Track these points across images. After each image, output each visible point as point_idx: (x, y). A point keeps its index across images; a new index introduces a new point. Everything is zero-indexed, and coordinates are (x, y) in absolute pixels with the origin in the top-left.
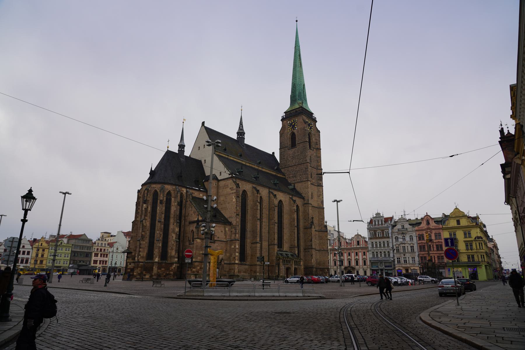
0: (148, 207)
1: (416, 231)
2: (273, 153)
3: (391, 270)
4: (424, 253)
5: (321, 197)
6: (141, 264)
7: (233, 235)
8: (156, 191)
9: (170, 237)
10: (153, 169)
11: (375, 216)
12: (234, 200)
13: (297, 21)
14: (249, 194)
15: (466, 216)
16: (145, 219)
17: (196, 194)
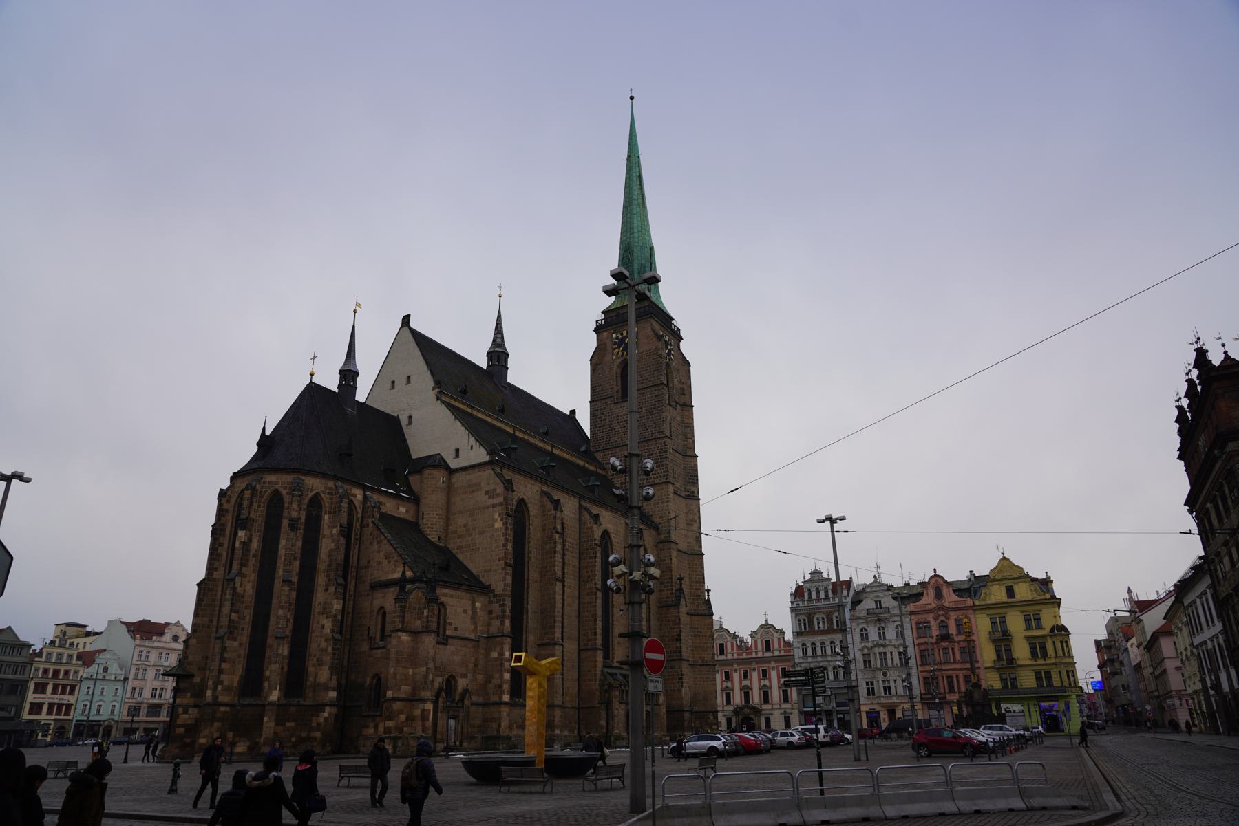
0: (250, 540)
1: (912, 613)
2: (573, 412)
5: (695, 525)
6: (223, 709)
7: (496, 623)
8: (277, 493)
9: (314, 627)
10: (268, 433)
11: (808, 577)
12: (499, 524)
13: (632, 98)
14: (533, 510)
15: (1028, 576)
16: (240, 574)
17: (390, 507)
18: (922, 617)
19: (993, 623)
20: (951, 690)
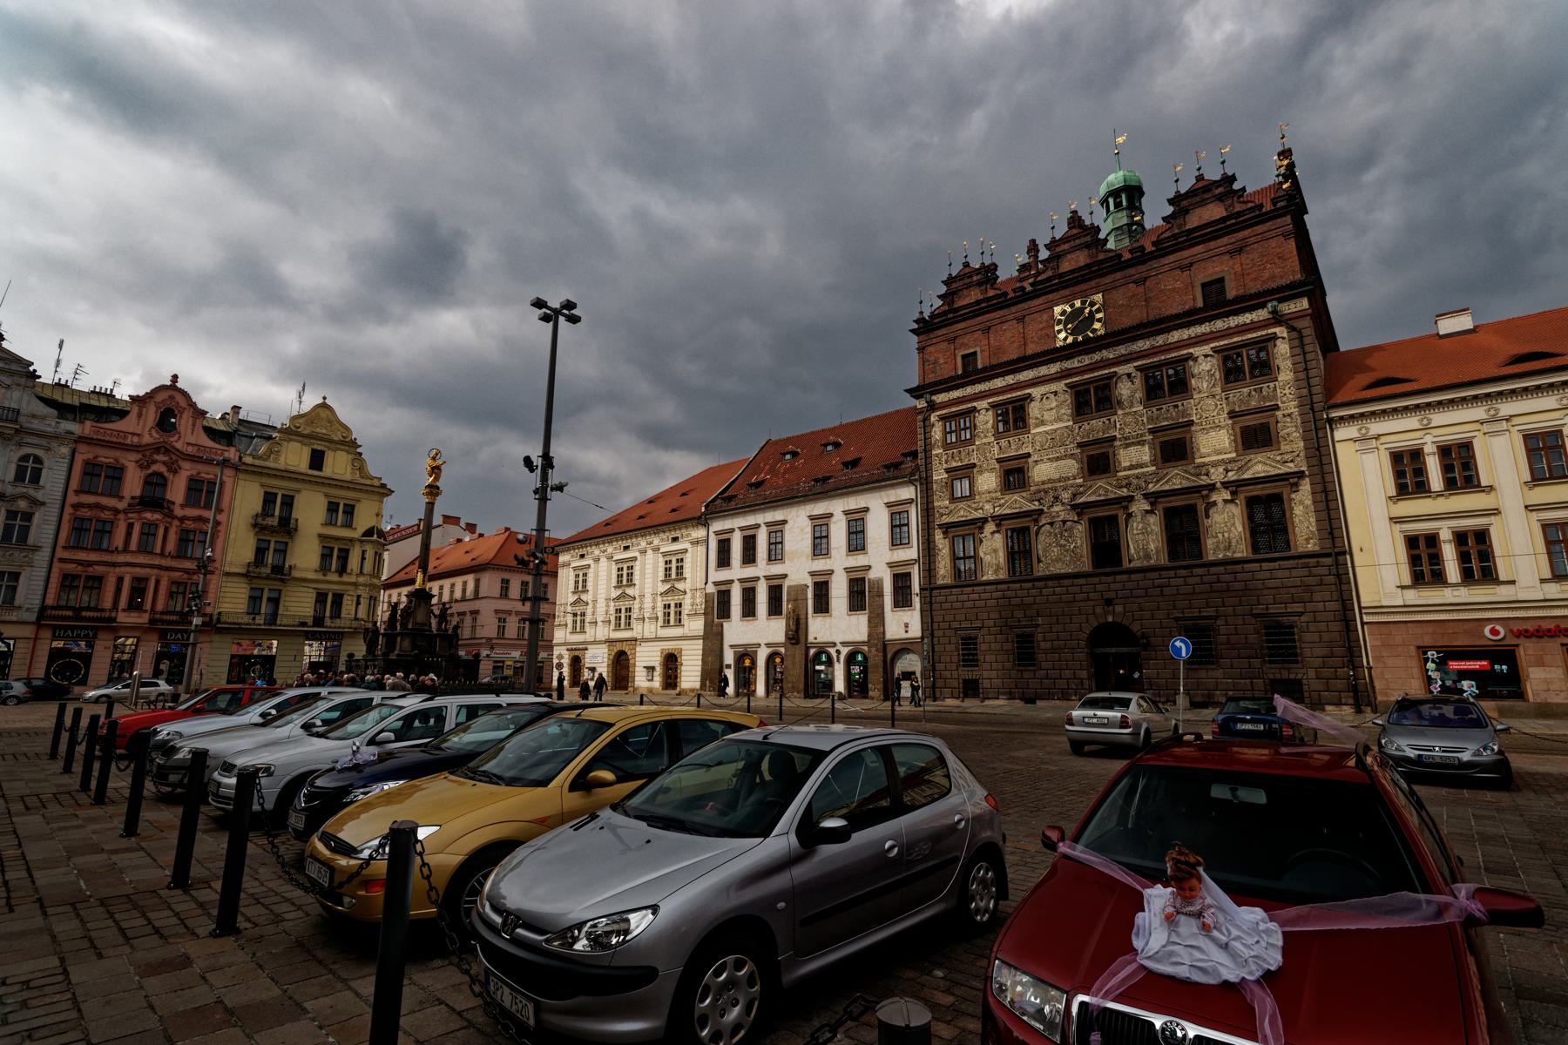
1: (81, 440)
4: (93, 557)
15: (353, 444)
19: (269, 499)
20: (134, 606)
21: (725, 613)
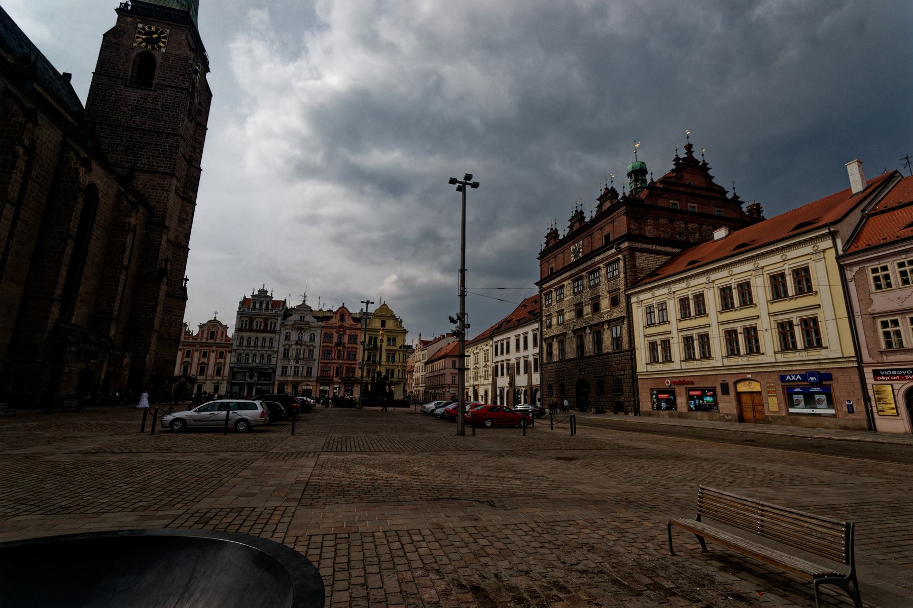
1: (323, 327)
3: (269, 384)
5: (186, 225)
15: (394, 316)
18: (329, 331)
21: (497, 375)
